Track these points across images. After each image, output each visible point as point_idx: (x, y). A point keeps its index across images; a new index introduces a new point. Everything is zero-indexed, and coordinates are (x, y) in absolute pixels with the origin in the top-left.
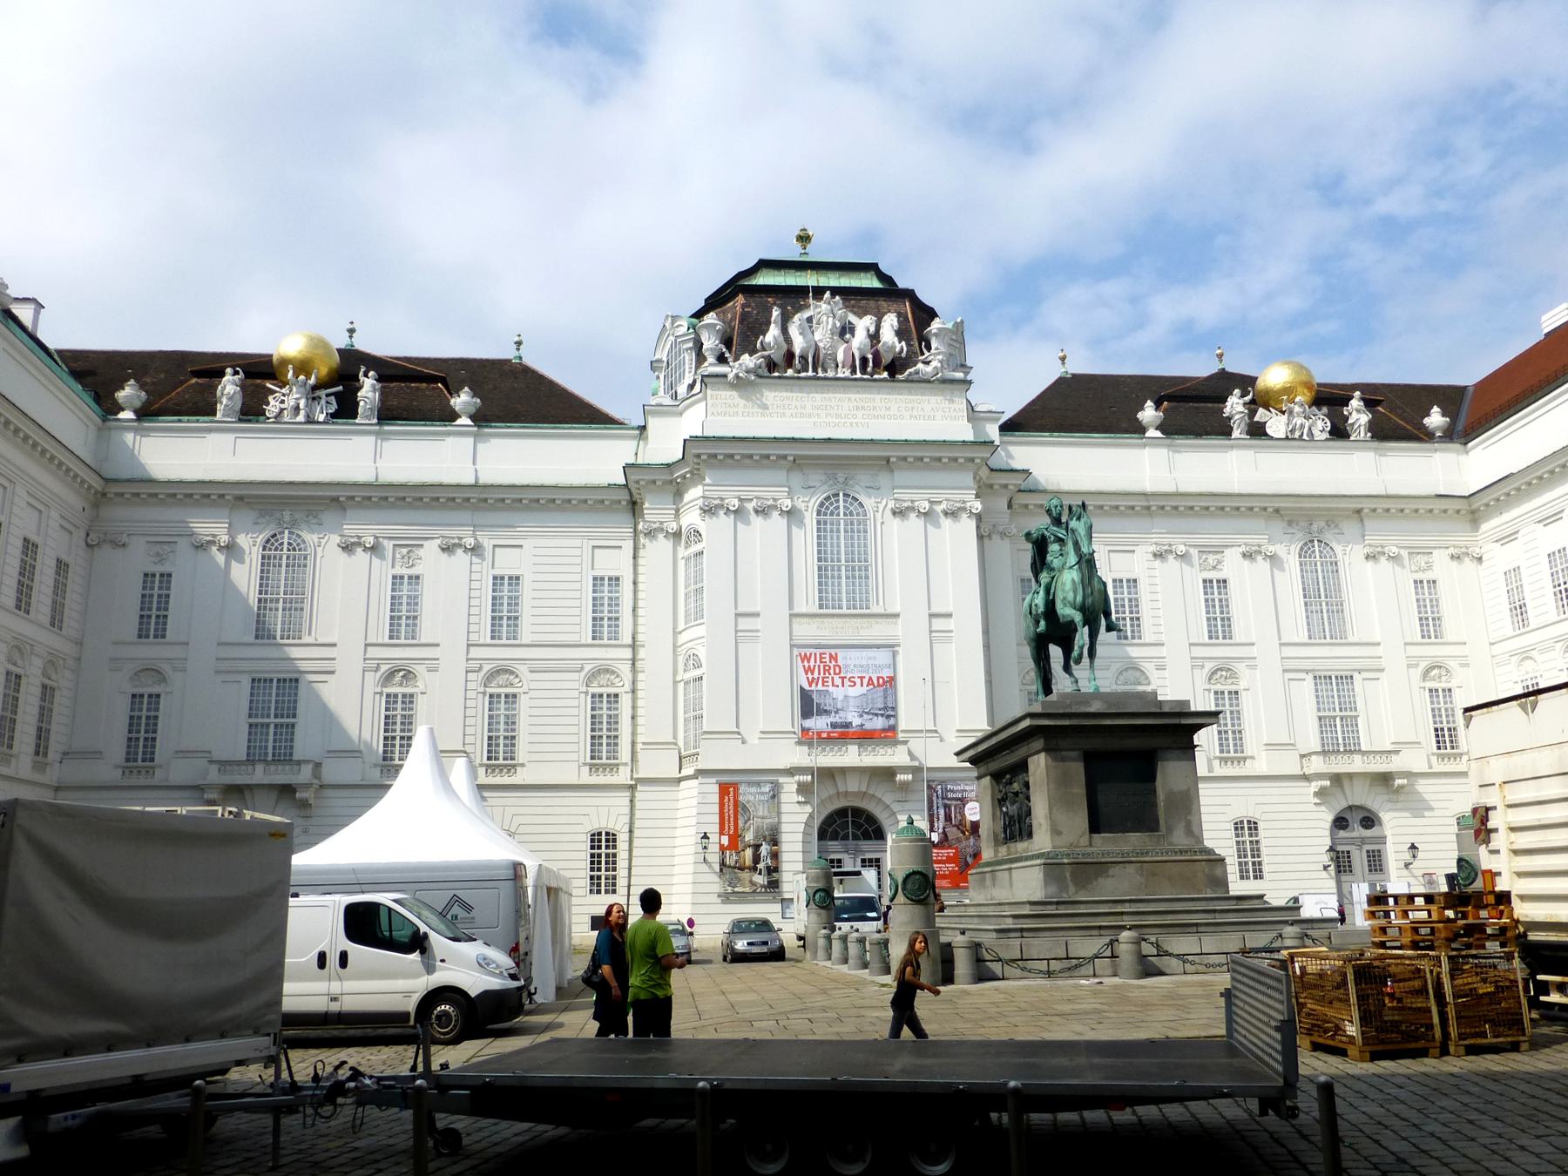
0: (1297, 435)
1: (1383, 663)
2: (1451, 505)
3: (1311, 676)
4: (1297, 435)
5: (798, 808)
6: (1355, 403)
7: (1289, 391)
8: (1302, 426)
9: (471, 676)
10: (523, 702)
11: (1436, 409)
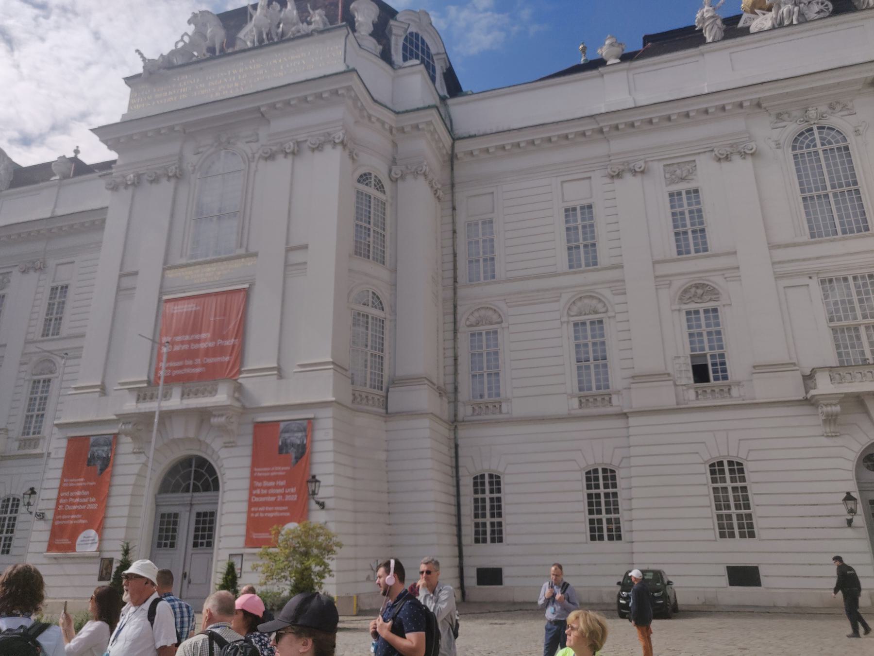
3: (814, 283)
5: (132, 458)
9: (24, 367)
10: (54, 386)
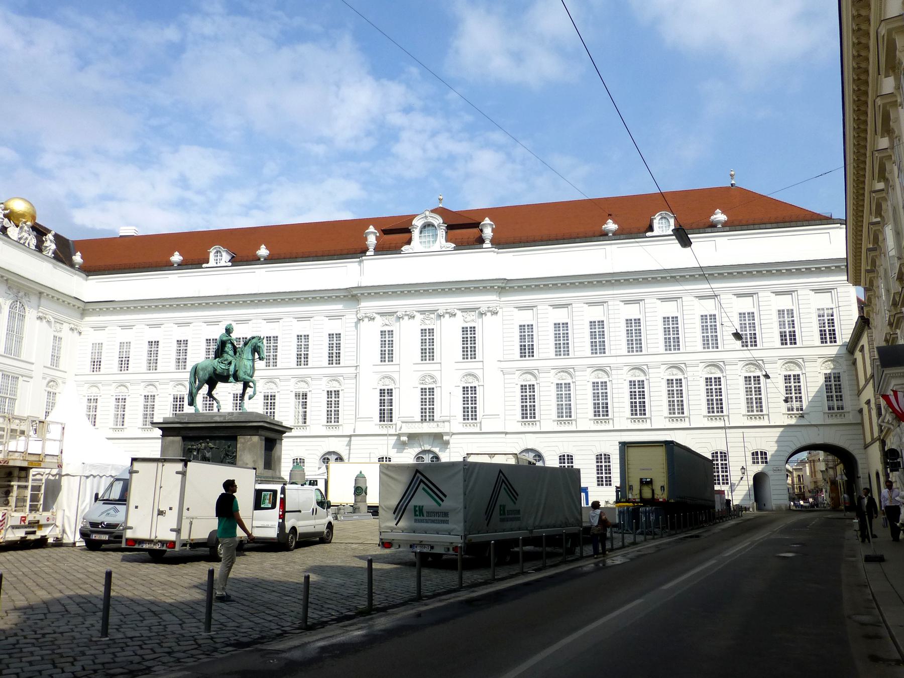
0: (22, 241)
1: (33, 374)
2: (78, 304)
4: (22, 241)
6: (50, 236)
7: (23, 215)
8: (27, 239)
11: (79, 254)
